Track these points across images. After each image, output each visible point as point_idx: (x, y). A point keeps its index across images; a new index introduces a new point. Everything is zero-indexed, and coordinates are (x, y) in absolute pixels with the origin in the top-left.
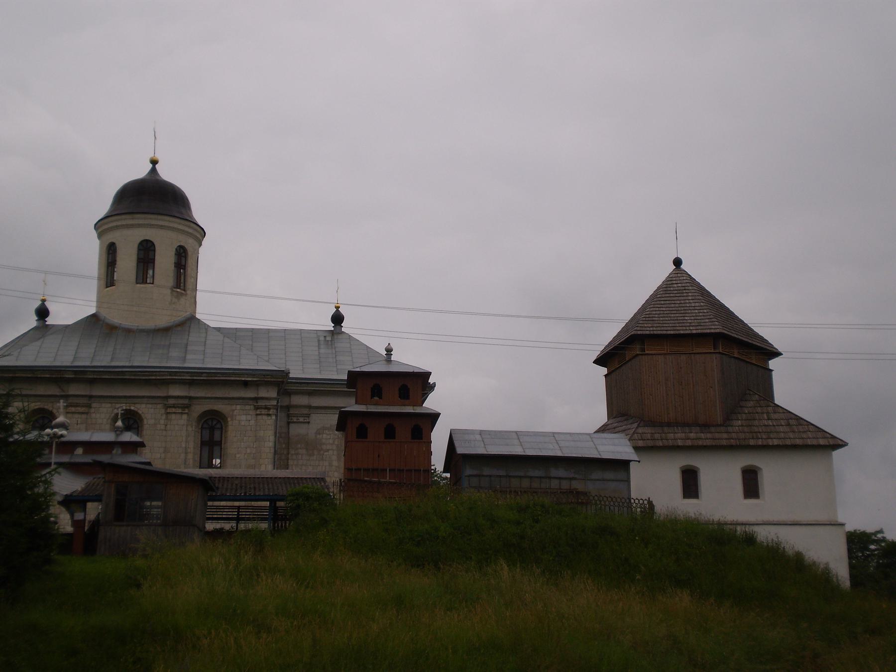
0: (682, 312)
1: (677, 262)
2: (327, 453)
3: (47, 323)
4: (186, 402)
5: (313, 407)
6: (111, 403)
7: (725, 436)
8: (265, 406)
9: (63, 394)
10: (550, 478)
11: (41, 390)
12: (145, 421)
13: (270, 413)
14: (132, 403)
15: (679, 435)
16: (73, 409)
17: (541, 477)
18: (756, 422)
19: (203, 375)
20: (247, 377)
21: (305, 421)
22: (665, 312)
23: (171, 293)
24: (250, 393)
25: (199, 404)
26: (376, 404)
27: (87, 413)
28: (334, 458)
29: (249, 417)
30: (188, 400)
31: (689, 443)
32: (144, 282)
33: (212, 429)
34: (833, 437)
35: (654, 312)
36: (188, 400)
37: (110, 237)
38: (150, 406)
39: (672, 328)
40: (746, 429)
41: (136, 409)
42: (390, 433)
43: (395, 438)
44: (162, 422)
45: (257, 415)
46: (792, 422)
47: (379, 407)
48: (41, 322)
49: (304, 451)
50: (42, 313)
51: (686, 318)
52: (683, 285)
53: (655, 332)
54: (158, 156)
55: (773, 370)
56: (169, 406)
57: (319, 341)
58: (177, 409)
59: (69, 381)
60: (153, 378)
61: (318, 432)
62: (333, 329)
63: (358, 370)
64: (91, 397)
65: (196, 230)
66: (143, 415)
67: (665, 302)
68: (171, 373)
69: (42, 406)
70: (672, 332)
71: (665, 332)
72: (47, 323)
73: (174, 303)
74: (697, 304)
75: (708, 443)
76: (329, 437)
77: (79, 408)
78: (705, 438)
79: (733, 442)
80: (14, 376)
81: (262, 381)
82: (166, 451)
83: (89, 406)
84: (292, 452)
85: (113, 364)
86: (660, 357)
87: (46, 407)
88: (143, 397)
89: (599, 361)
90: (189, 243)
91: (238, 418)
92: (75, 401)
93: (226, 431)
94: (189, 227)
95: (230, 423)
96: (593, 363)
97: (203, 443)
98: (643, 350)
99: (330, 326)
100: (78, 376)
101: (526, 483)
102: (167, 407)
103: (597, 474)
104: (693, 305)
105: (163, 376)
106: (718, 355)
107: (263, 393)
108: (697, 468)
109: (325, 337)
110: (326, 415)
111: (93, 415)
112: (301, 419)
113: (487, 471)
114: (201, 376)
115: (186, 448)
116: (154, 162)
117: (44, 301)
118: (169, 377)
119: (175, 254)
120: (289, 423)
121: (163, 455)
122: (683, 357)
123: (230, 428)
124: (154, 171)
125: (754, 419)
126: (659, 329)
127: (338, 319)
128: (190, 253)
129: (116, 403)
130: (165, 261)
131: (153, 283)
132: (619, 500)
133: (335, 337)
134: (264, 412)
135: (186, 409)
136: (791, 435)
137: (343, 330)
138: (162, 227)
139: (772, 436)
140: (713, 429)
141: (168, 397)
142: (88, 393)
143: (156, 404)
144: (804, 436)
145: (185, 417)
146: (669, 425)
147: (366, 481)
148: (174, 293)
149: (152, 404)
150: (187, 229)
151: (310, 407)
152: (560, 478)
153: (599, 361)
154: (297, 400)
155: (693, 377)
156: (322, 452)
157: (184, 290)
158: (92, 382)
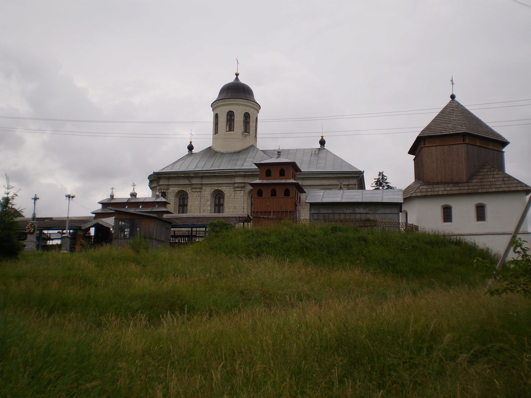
0: (448, 123)
1: (453, 97)
3: (193, 152)
4: (243, 185)
5: (304, 185)
6: (211, 187)
7: (466, 188)
10: (356, 213)
11: (181, 182)
15: (440, 189)
16: (195, 190)
17: (350, 213)
18: (486, 180)
22: (439, 124)
23: (242, 135)
26: (269, 179)
27: (201, 192)
31: (445, 193)
32: (230, 130)
34: (526, 186)
35: (433, 124)
37: (217, 111)
38: (227, 187)
39: (439, 132)
40: (479, 184)
41: (221, 189)
42: (274, 193)
43: (276, 196)
46: (505, 179)
47: (269, 181)
48: (190, 152)
50: (190, 148)
51: (449, 126)
52: (453, 108)
53: (430, 135)
54: (239, 72)
55: (504, 152)
57: (312, 153)
58: (239, 188)
59: (192, 177)
60: (228, 174)
62: (320, 147)
63: (259, 162)
64: (202, 184)
65: (254, 105)
67: (440, 118)
68: (235, 172)
69: (182, 189)
70: (439, 134)
71: (435, 134)
72: (193, 152)
73: (243, 139)
74: (457, 118)
75: (456, 192)
77: (197, 190)
78: (456, 190)
79: (470, 191)
80: (169, 176)
85: (211, 169)
86: (434, 147)
87: (183, 190)
88: (224, 183)
89: (411, 152)
90: (251, 111)
92: (195, 186)
94: (250, 103)
96: (408, 153)
98: (425, 144)
99: (319, 146)
100: (195, 175)
101: (342, 217)
103: (381, 211)
104: (455, 118)
106: (465, 145)
108: (451, 206)
109: (315, 151)
113: (322, 211)
114: (249, 173)
115: (243, 206)
116: (237, 75)
117: (191, 142)
119: (244, 116)
122: (446, 147)
124: (237, 79)
125: (485, 178)
126: (432, 132)
127: (322, 142)
128: (251, 116)
130: (239, 119)
131: (234, 131)
132: (389, 224)
133: (320, 151)
136: (503, 186)
137: (325, 147)
138: (237, 104)
139: (492, 187)
140: (460, 185)
141: (235, 183)
142: (201, 183)
143: (229, 186)
144: (510, 186)
145: (242, 192)
146: (437, 183)
147: (261, 217)
148: (244, 135)
150: (249, 104)
152: (360, 213)
153: (411, 152)
155: (451, 157)
157: (249, 133)
158: (202, 177)
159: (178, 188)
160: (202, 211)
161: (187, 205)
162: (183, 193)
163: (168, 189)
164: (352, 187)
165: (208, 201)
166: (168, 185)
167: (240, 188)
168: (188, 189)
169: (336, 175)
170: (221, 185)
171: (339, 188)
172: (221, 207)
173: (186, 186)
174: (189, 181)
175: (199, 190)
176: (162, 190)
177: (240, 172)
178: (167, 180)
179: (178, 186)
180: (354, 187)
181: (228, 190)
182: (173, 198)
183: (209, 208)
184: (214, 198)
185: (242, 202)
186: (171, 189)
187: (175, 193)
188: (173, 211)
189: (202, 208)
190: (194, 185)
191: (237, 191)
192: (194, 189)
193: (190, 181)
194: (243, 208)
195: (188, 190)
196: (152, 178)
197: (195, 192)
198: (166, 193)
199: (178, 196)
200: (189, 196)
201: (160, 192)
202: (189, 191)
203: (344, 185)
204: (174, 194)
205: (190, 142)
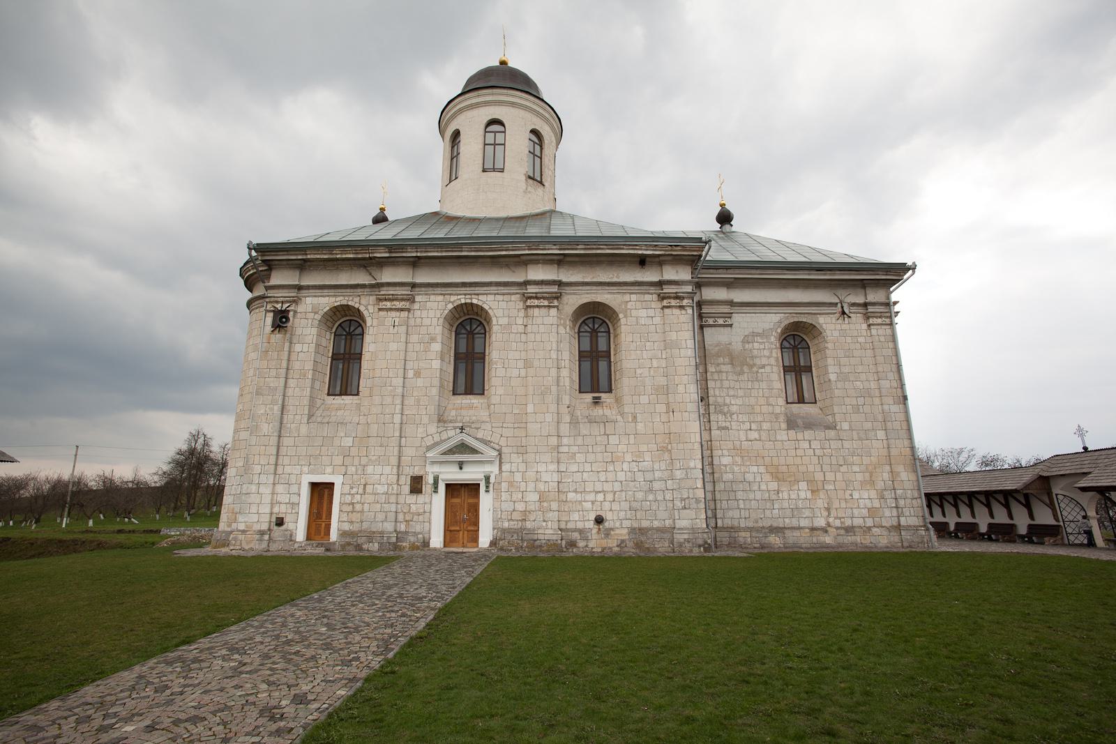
2: (763, 370)
4: (555, 289)
6: (444, 295)
8: (676, 293)
11: (344, 278)
12: (494, 321)
13: (684, 304)
14: (475, 294)
16: (388, 304)
19: (578, 247)
20: (647, 250)
21: (727, 323)
23: (526, 180)
24: (650, 275)
25: (574, 294)
27: (409, 310)
28: (775, 377)
29: (651, 312)
30: (557, 287)
33: (594, 333)
36: (557, 287)
38: (498, 297)
41: (480, 303)
44: (520, 321)
45: (664, 307)
49: (728, 368)
56: (530, 296)
58: (542, 300)
59: (382, 263)
60: (504, 253)
61: (746, 340)
64: (414, 285)
66: (490, 311)
73: (529, 192)
76: (762, 347)
77: (395, 303)
80: (304, 257)
81: (668, 255)
82: (528, 364)
83: (412, 300)
84: (711, 369)
87: (350, 303)
91: (634, 313)
92: (392, 291)
93: (616, 336)
95: (623, 321)
97: (582, 355)
99: (717, 226)
102: (526, 297)
105: (519, 250)
107: (670, 273)
110: (754, 315)
111: (418, 313)
112: (721, 321)
114: (576, 249)
117: (382, 210)
118: (527, 252)
120: (702, 327)
121: (523, 372)
123: (623, 328)
127: (725, 218)
129: (450, 294)
130: (517, 142)
134: (673, 303)
135: (556, 301)
138: (513, 104)
141: (527, 283)
142: (409, 280)
145: (553, 312)
149: (504, 294)
150: (541, 111)
151: (731, 303)
154: (709, 294)
156: (755, 369)
157: (541, 182)
158: (415, 263)
159: (333, 299)
160: (410, 374)
161: (359, 357)
162: (348, 318)
163: (296, 301)
164: (878, 310)
165: (433, 339)
166: (299, 288)
167: (544, 298)
168: (364, 301)
169: (830, 275)
171: (838, 315)
172: (477, 366)
173: (359, 290)
175: (403, 303)
176: (277, 302)
177: (547, 246)
178: (297, 273)
179: (333, 291)
180: (882, 310)
181: (503, 305)
182: (314, 331)
183: (436, 364)
184: (453, 334)
185: (554, 346)
186: (309, 300)
187: (321, 313)
188: (311, 372)
189: (411, 363)
190: (385, 288)
191: (536, 310)
192: (386, 300)
193: (373, 277)
194: (555, 365)
195: (366, 304)
196: (250, 270)
197: (391, 309)
198: (291, 314)
199: (329, 324)
200: (369, 323)
201: (271, 311)
202: (370, 307)
203: (854, 305)
204: (318, 317)
205: (381, 209)
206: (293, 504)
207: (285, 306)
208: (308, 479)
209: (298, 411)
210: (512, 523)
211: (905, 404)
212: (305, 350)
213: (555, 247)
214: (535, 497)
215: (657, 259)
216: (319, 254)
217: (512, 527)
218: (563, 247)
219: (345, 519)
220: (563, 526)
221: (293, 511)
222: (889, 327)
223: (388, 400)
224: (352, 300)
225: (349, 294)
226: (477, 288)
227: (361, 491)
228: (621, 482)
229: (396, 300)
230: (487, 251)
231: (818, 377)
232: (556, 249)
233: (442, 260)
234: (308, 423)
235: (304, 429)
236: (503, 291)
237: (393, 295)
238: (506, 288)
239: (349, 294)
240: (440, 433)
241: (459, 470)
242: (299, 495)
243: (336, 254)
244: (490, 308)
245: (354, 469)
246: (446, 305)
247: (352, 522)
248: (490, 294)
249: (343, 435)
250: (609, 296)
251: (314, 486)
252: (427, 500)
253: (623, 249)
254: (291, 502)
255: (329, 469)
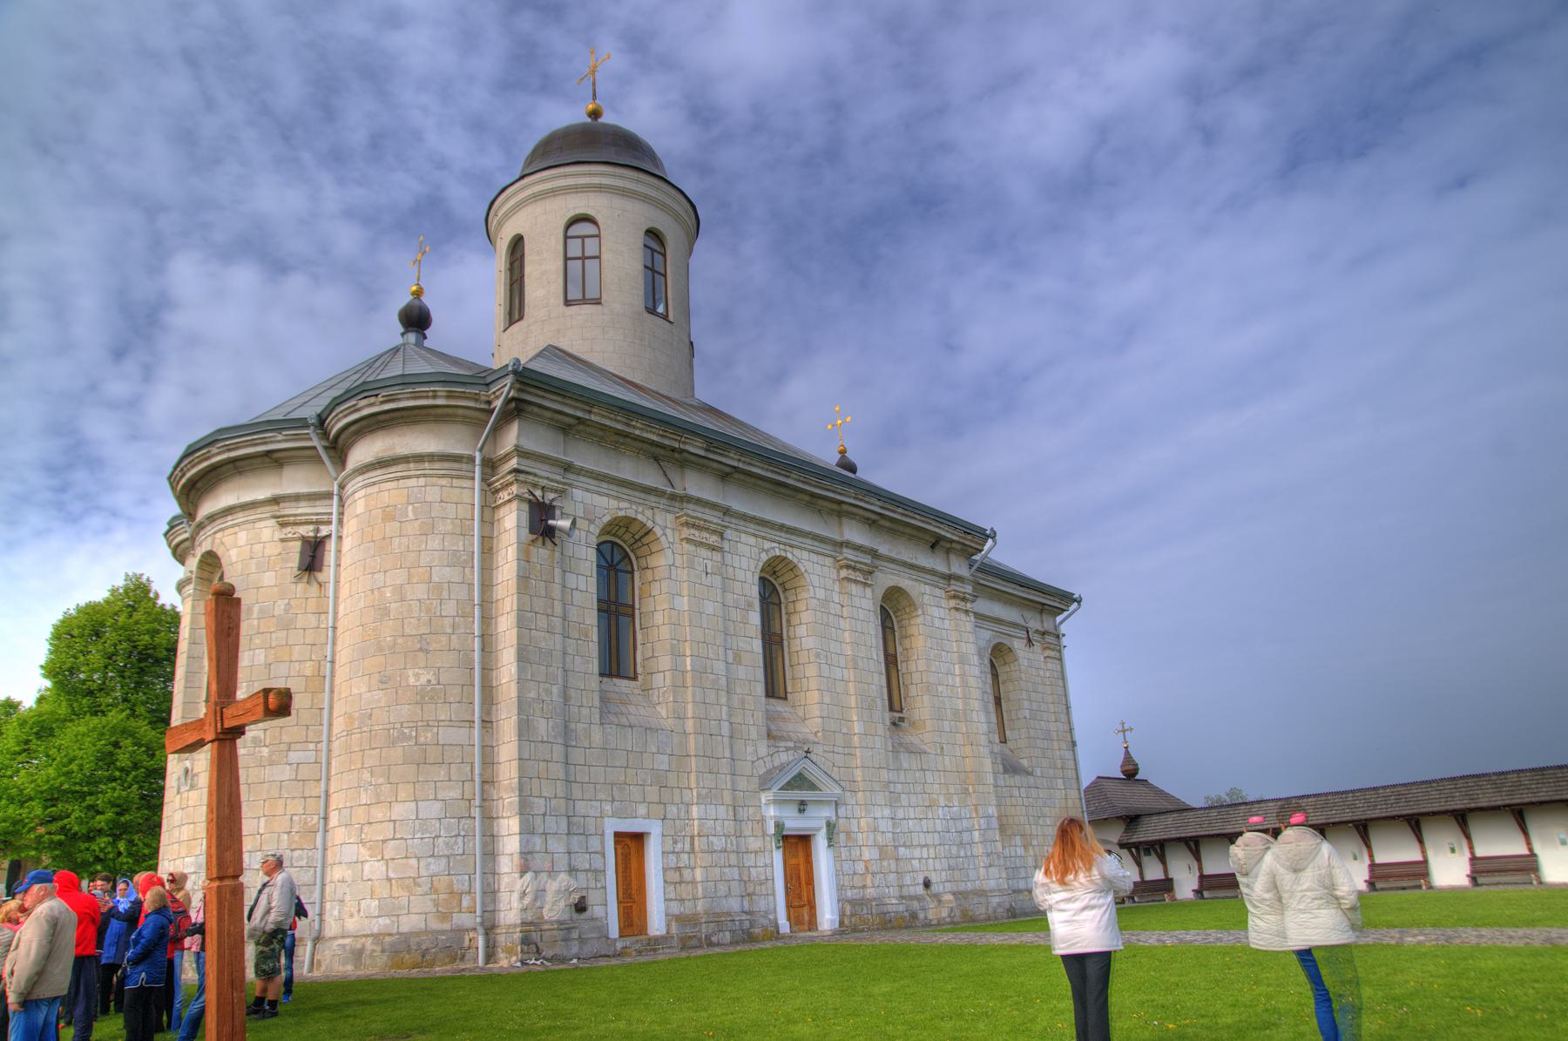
4: (867, 559)
9: (669, 490)
38: (814, 557)
41: (795, 561)
59: (683, 461)
69: (631, 514)
87: (640, 517)
100: (711, 456)
129: (764, 538)
159: (614, 503)
168: (660, 518)
170: (796, 540)
173: (653, 498)
174: (666, 481)
176: (535, 485)
178: (561, 437)
186: (578, 494)
190: (691, 506)
196: (435, 397)
202: (669, 532)
206: (596, 871)
207: (551, 496)
208: (612, 826)
209: (584, 701)
210: (855, 891)
211: (1073, 751)
212: (582, 587)
213: (878, 503)
214: (875, 853)
215: (948, 545)
216: (610, 419)
217: (855, 897)
218: (887, 505)
219: (672, 896)
220: (905, 892)
221: (599, 886)
222: (1058, 662)
223: (711, 697)
224: (643, 513)
225: (638, 500)
226: (793, 537)
227: (687, 847)
228: (939, 832)
229: (707, 529)
230: (815, 486)
231: (1010, 711)
232: (878, 506)
233: (760, 482)
234: (601, 724)
235: (597, 736)
236: (819, 549)
237: (705, 521)
238: (822, 545)
239: (638, 500)
240: (772, 755)
241: (797, 814)
242: (604, 854)
243: (634, 427)
244: (806, 571)
245: (674, 809)
246: (760, 553)
247: (682, 900)
248: (805, 549)
249: (654, 749)
250: (910, 583)
251: (618, 835)
252: (768, 862)
253: (930, 524)
254: (592, 868)
255: (642, 810)
